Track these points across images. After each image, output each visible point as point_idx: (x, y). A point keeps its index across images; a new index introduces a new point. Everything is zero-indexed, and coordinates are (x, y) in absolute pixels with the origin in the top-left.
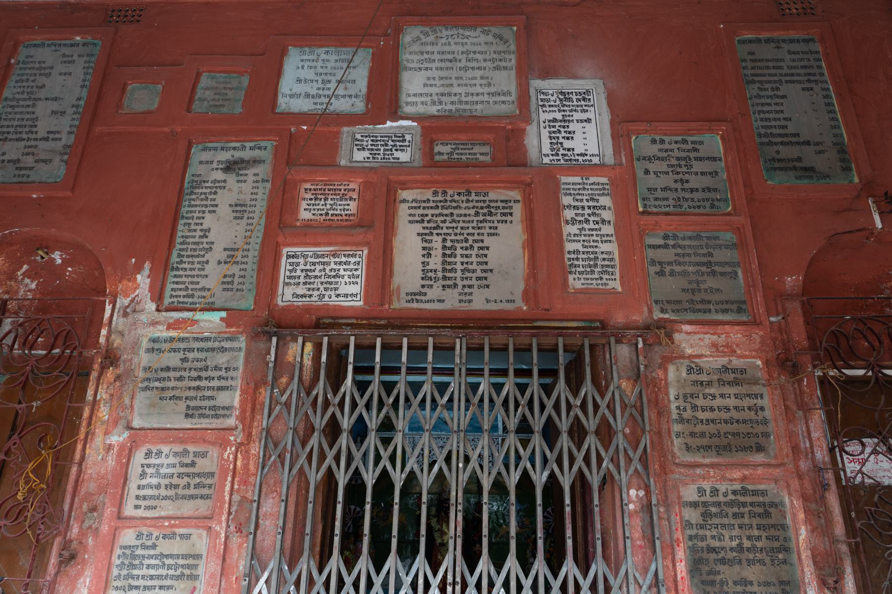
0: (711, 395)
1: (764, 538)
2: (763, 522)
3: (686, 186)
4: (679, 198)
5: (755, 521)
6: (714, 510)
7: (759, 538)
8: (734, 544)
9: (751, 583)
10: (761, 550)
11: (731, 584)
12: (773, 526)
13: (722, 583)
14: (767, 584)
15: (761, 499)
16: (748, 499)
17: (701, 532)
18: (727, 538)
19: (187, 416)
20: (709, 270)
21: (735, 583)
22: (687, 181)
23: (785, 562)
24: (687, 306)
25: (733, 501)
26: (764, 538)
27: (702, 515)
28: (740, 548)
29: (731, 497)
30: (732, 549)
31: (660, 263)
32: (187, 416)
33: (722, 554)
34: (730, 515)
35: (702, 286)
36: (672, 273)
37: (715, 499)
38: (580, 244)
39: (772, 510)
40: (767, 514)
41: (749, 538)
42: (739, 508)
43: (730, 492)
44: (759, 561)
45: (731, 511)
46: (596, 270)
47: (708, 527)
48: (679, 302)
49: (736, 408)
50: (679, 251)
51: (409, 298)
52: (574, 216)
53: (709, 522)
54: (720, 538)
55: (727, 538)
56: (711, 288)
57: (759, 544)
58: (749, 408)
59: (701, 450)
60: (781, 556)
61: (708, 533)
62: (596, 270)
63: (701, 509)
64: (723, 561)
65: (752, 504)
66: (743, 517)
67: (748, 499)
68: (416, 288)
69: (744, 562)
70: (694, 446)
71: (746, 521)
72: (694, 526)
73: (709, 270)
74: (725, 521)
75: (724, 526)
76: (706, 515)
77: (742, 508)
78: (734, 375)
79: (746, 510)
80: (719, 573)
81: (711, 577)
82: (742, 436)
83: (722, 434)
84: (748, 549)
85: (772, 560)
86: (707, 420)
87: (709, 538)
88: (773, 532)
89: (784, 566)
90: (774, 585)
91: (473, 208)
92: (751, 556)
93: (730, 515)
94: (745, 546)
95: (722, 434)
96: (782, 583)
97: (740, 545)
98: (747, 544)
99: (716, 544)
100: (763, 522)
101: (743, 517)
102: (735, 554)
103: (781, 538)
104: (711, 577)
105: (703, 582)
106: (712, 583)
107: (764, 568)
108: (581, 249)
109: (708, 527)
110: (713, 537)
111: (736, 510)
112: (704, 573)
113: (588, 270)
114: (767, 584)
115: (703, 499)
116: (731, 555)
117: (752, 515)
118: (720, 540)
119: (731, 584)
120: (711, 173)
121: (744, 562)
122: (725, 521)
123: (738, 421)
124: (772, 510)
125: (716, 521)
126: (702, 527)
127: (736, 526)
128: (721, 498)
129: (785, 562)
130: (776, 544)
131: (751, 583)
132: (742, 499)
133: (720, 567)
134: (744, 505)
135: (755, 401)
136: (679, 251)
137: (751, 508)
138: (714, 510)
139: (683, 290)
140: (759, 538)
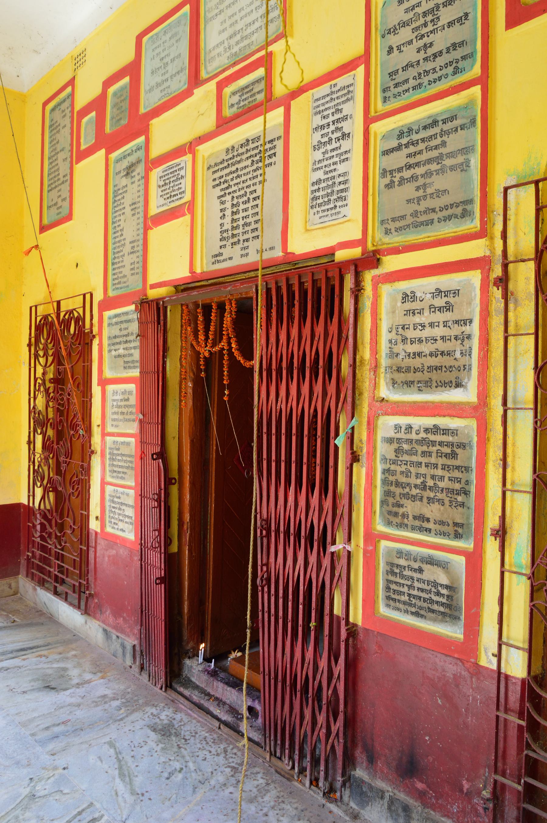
0: (421, 325)
1: (446, 479)
2: (449, 462)
3: (430, 52)
4: (420, 74)
5: (441, 461)
6: (406, 447)
7: (442, 478)
8: (419, 482)
9: (428, 520)
10: (442, 491)
11: (411, 517)
12: (458, 468)
13: (404, 516)
14: (442, 523)
15: (450, 439)
16: (438, 438)
17: (393, 467)
18: (413, 474)
19: (125, 368)
20: (439, 167)
21: (415, 518)
22: (431, 44)
23: (463, 505)
24: (409, 220)
25: (424, 439)
26: (446, 479)
27: (396, 451)
28: (424, 487)
29: (423, 435)
30: (416, 486)
31: (391, 172)
32: (125, 368)
33: (407, 490)
34: (419, 452)
35: (429, 191)
36: (402, 181)
37: (408, 436)
38: (321, 172)
39: (459, 451)
40: (454, 455)
41: (433, 477)
42: (428, 446)
43: (422, 430)
44: (438, 500)
45: (420, 449)
46: (332, 198)
47: (399, 463)
48: (403, 217)
49: (442, 338)
50: (412, 149)
51: (213, 260)
52: (319, 138)
53: (401, 458)
54: (407, 474)
55: (413, 474)
56: (438, 191)
57: (441, 484)
58: (456, 338)
59: (405, 386)
60: (460, 499)
61: (399, 469)
62: (332, 198)
63: (395, 446)
64: (406, 496)
65: (441, 444)
66: (430, 456)
67: (438, 438)
68: (217, 251)
69: (425, 500)
70: (399, 382)
71: (433, 460)
72: (388, 461)
73: (439, 167)
74: (414, 458)
75: (412, 463)
76: (398, 451)
77: (430, 447)
78: (445, 299)
79: (434, 449)
80: (402, 506)
81: (395, 509)
82: (444, 369)
83: (426, 368)
84: (431, 488)
85: (451, 502)
86: (414, 354)
87: (398, 473)
88: (456, 474)
89: (460, 509)
90: (448, 525)
91: (247, 158)
92: (432, 495)
93: (419, 452)
94: (427, 484)
95: (426, 368)
96: (456, 524)
97: (424, 483)
98: (430, 483)
99: (403, 480)
100: (449, 462)
101: (430, 456)
102: (418, 491)
103: (463, 481)
104: (395, 509)
105: (390, 513)
106: (396, 514)
107: (442, 508)
108: (323, 177)
109: (399, 463)
110: (402, 473)
111: (425, 448)
112: (390, 504)
113: (326, 199)
114: (442, 523)
115: (399, 436)
116: (414, 492)
117: (440, 455)
118: (407, 476)
119: (411, 517)
120: (459, 20)
121: (425, 500)
122: (414, 458)
123: (442, 353)
124: (459, 451)
125: (406, 457)
126: (394, 462)
127: (423, 465)
128: (414, 436)
129: (463, 505)
130: (457, 486)
131: (428, 520)
132: (432, 437)
133: (404, 501)
134: (433, 443)
135: (464, 328)
136: (412, 149)
137: (438, 447)
138: (406, 447)
139: (409, 201)
140: (442, 478)
